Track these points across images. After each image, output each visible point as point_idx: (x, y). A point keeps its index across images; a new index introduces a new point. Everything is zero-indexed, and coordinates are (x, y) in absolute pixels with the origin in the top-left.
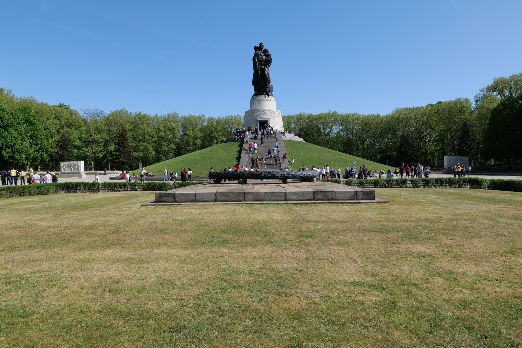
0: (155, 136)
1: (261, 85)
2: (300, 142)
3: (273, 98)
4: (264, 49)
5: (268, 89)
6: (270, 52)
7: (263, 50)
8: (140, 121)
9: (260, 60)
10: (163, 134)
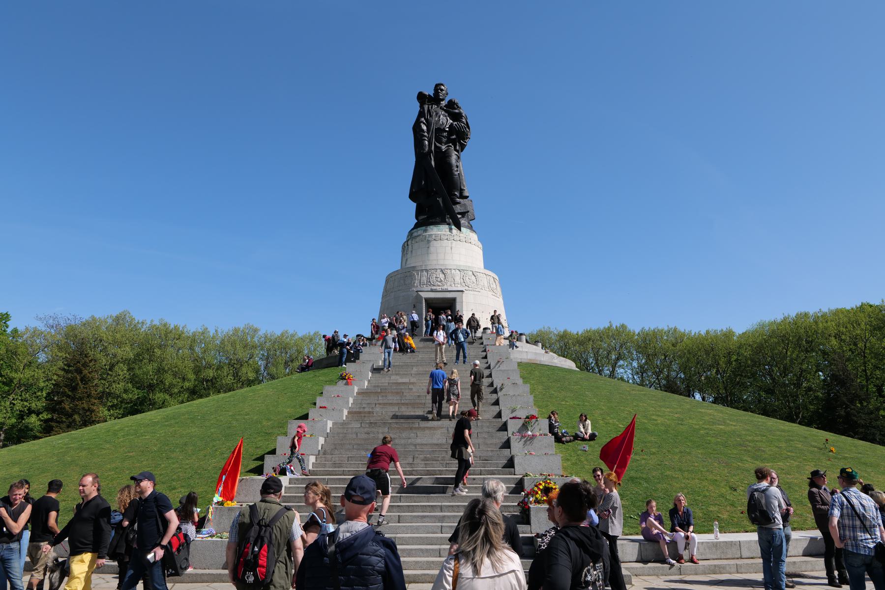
0: (192, 376)
2: (570, 371)
4: (447, 99)
5: (458, 209)
7: (443, 103)
9: (433, 127)
10: (211, 373)
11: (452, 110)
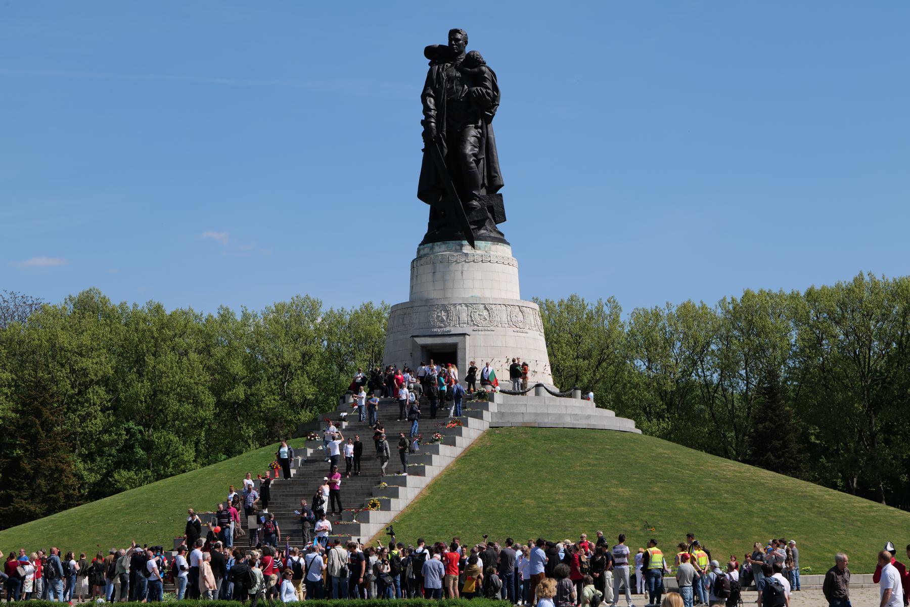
0: (209, 399)
1: (460, 197)
3: (502, 251)
6: (492, 60)
7: (462, 57)
8: (142, 342)
10: (240, 392)
11: (474, 70)
